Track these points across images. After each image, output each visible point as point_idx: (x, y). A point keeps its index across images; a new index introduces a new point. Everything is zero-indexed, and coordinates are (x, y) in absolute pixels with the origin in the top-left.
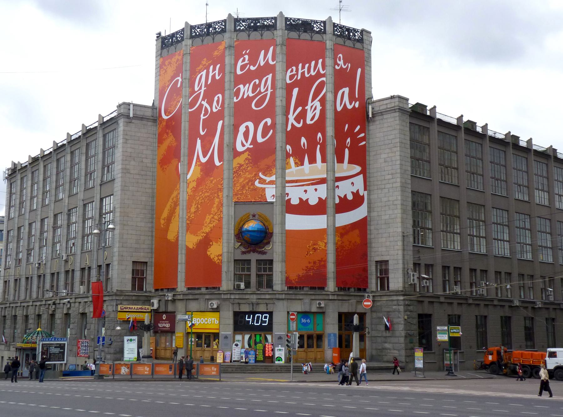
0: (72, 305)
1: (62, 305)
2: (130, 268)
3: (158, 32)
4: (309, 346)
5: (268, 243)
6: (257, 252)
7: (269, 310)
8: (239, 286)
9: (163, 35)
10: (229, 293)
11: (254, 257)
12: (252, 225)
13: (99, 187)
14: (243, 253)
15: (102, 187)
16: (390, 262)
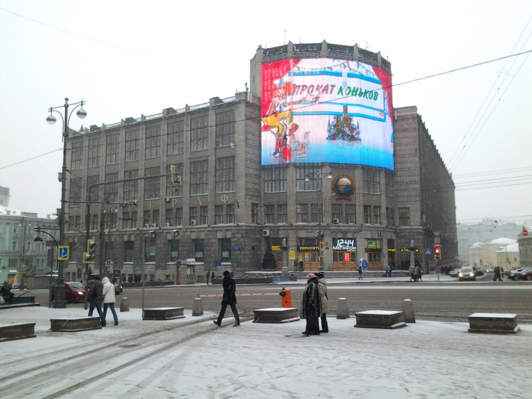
0: (181, 233)
1: (163, 234)
2: (250, 208)
3: (259, 45)
4: (375, 260)
5: (353, 194)
6: (346, 199)
7: (355, 237)
8: (336, 221)
9: (263, 47)
10: (328, 225)
11: (344, 202)
12: (345, 181)
13: (213, 151)
14: (337, 199)
15: (217, 150)
16: (411, 209)
